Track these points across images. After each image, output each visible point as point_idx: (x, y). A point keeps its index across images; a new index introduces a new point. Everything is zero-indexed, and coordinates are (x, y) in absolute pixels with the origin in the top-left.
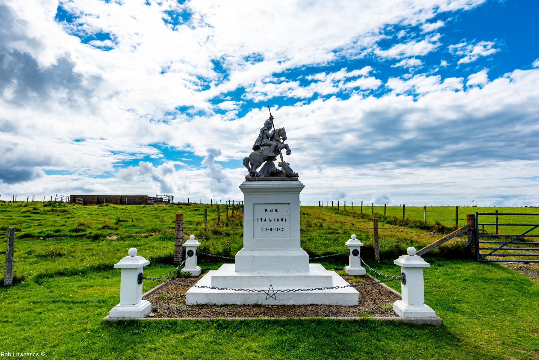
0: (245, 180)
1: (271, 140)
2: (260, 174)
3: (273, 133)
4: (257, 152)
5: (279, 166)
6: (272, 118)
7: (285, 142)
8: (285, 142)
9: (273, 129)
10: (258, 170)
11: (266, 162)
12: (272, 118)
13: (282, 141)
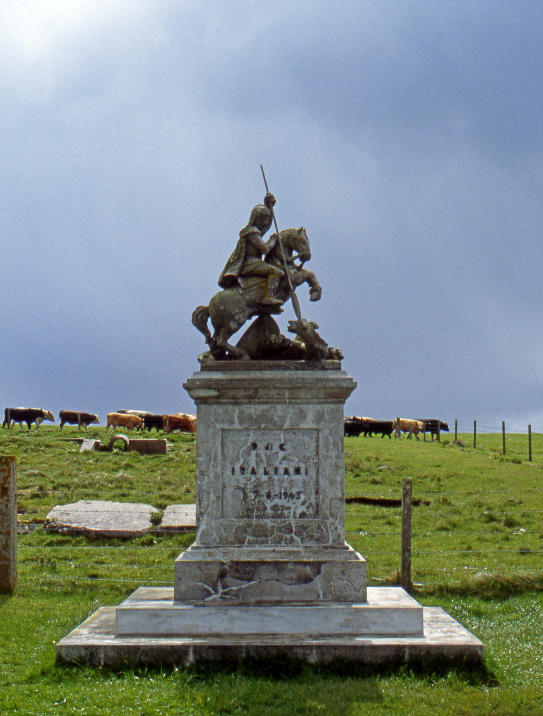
0: (198, 366)
1: (268, 260)
2: (238, 350)
3: (273, 243)
4: (229, 292)
5: (291, 330)
6: (270, 201)
7: (307, 267)
8: (307, 267)
9: (272, 231)
10: (233, 341)
11: (255, 318)
12: (270, 201)
13: (297, 262)
